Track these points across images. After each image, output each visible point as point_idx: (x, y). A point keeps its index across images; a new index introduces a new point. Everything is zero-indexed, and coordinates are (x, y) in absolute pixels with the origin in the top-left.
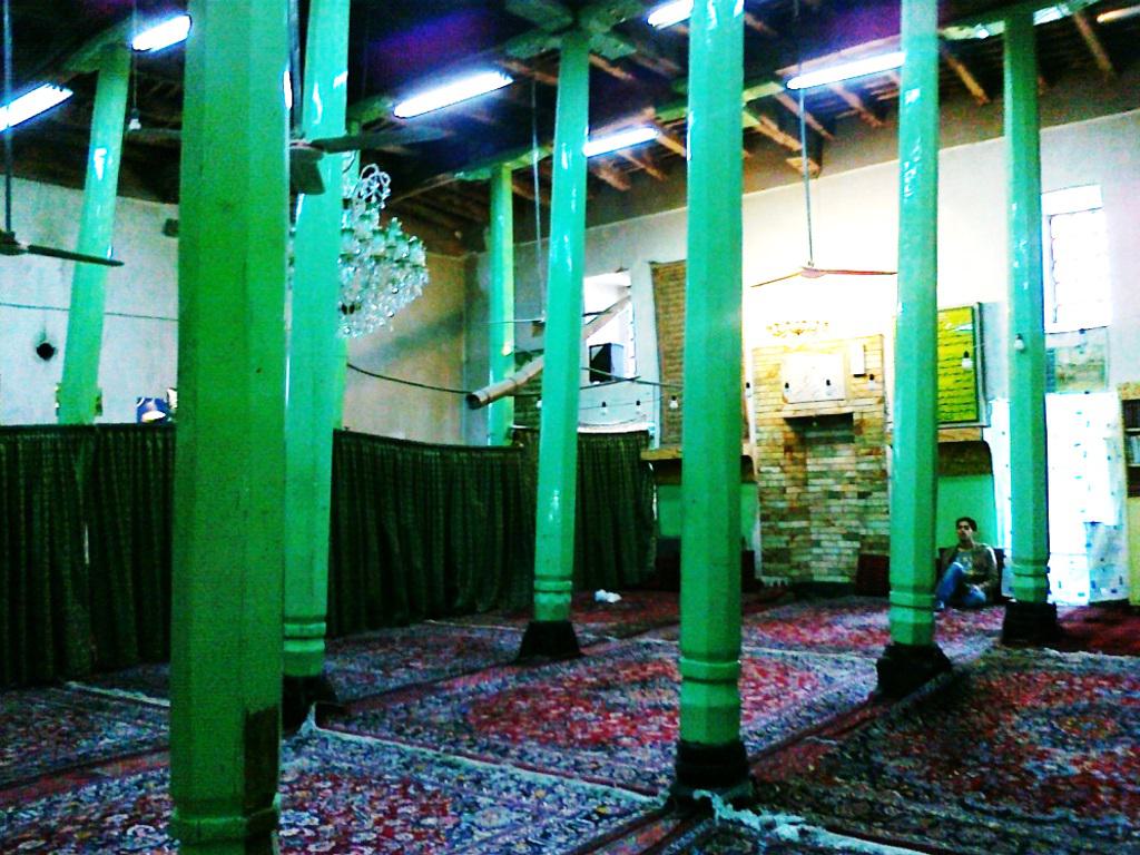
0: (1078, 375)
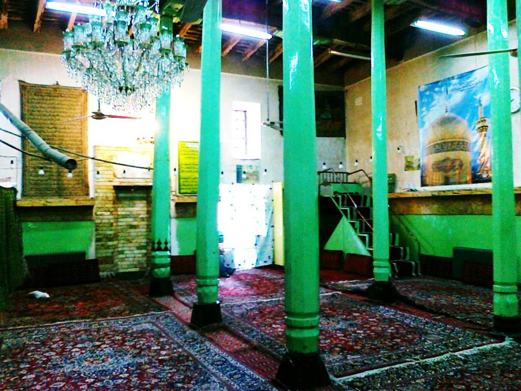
0: (250, 177)
